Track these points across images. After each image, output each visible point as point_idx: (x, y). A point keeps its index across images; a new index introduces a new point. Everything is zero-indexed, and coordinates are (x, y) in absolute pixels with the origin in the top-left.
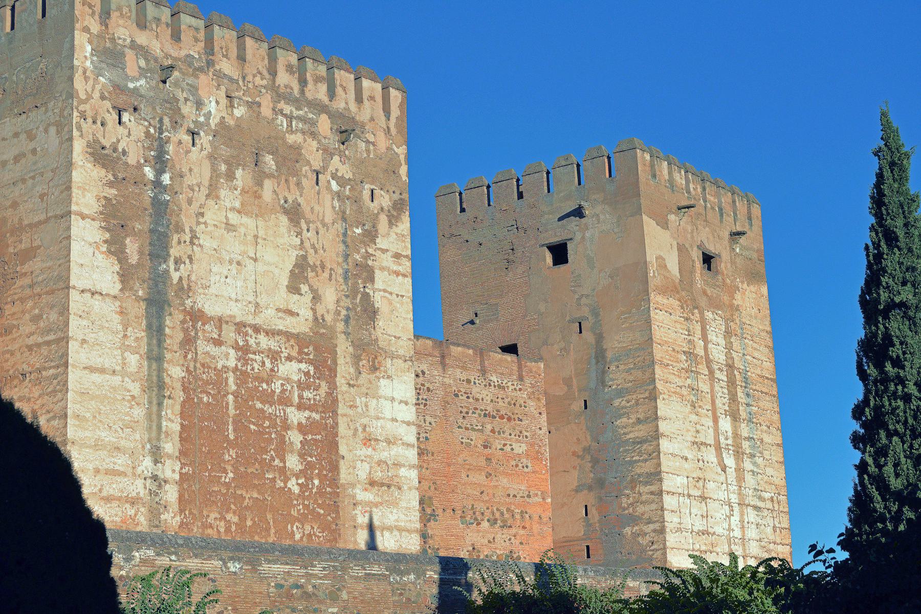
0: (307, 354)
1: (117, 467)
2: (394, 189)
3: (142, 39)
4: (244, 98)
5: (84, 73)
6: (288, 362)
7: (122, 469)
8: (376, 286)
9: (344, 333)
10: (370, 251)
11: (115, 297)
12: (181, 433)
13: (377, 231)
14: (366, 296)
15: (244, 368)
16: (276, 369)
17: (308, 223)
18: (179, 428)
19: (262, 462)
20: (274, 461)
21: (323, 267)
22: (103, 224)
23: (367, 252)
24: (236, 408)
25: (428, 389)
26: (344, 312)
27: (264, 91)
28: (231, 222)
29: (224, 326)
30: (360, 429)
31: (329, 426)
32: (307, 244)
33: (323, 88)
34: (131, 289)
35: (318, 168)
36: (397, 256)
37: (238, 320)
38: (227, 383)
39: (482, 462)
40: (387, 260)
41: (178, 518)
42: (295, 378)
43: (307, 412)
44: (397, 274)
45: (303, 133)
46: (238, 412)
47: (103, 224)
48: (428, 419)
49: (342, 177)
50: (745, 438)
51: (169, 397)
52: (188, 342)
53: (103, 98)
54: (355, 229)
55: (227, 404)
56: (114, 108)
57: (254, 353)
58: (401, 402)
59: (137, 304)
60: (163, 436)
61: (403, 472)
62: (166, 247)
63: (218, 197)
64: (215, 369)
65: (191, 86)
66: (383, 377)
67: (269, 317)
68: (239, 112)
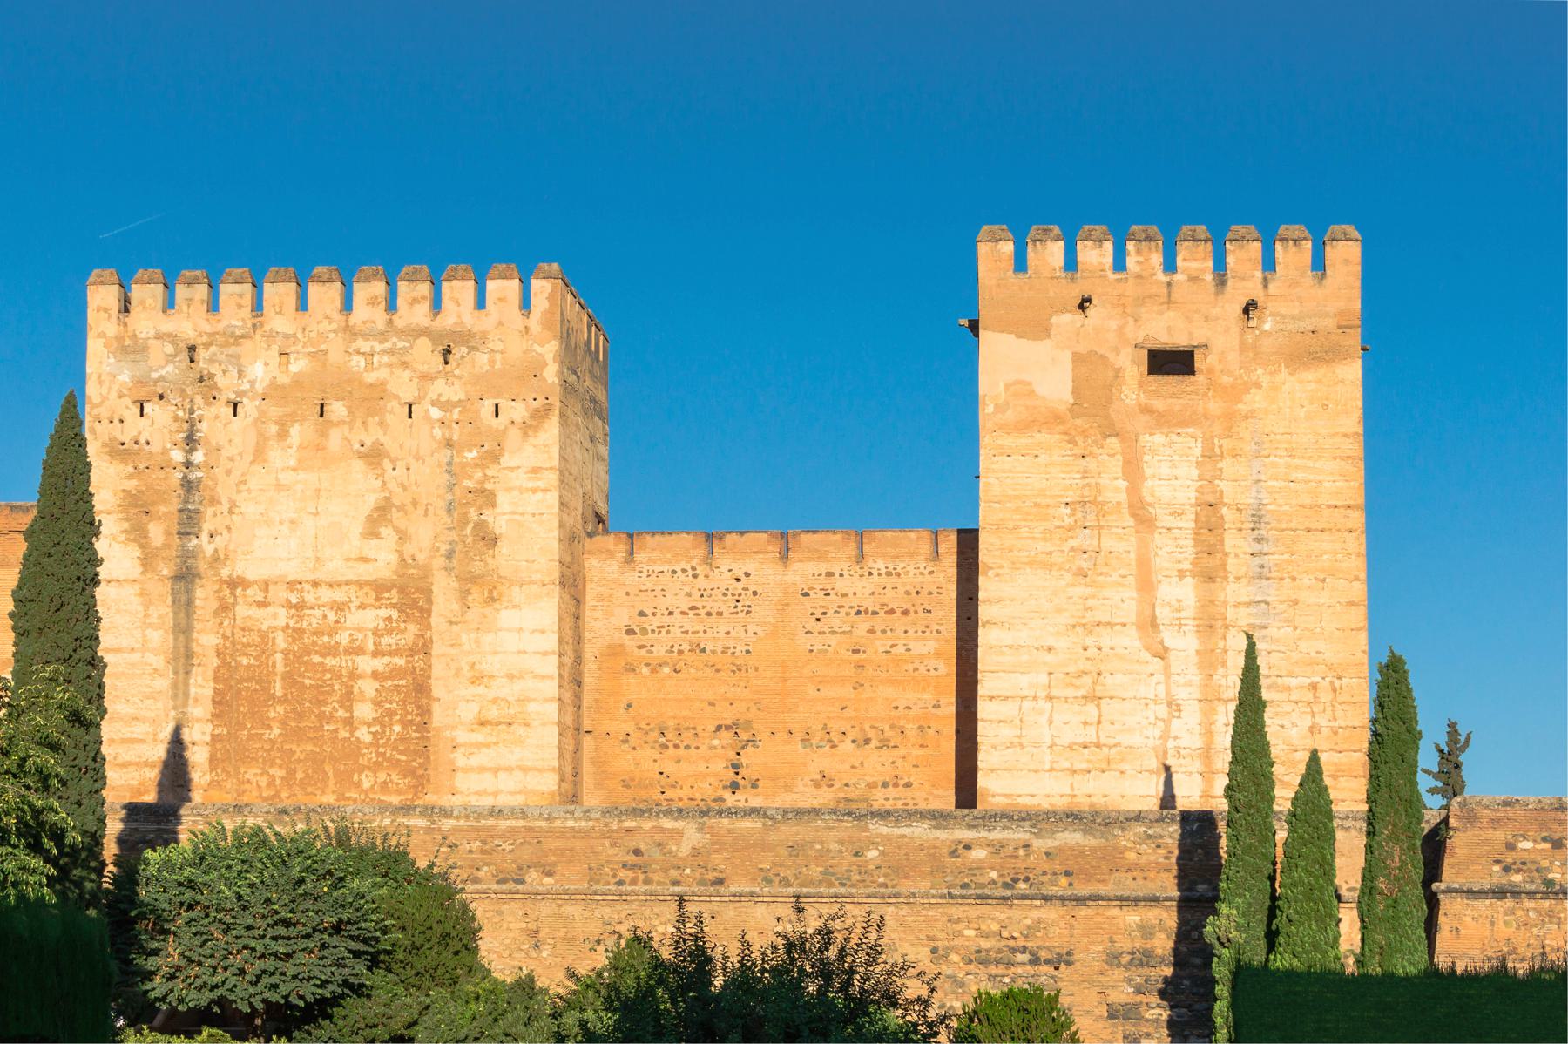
0: (388, 599)
1: (135, 736)
2: (534, 396)
3: (168, 325)
4: (304, 350)
5: (99, 377)
6: (361, 611)
7: (140, 737)
8: (498, 510)
9: (446, 569)
10: (489, 473)
11: (135, 581)
12: (213, 697)
13: (503, 449)
14: (481, 525)
15: (298, 625)
16: (342, 620)
17: (392, 461)
18: (209, 692)
19: (321, 717)
20: (337, 711)
21: (415, 503)
22: (121, 516)
23: (485, 475)
24: (286, 665)
25: (755, 593)
26: (444, 548)
27: (332, 335)
28: (283, 482)
29: (271, 588)
30: (466, 668)
31: (417, 670)
32: (392, 485)
33: (424, 308)
34: (154, 570)
35: (410, 400)
36: (535, 470)
37: (290, 578)
38: (274, 644)
39: (849, 671)
40: (521, 479)
41: (208, 778)
42: (371, 625)
43: (386, 657)
44: (534, 491)
45: (390, 366)
46: (288, 669)
47: (121, 516)
48: (751, 628)
49: (448, 401)
50: (1237, 605)
51: (199, 665)
52: (224, 608)
53: (121, 396)
54: (466, 454)
55: (274, 662)
56: (135, 402)
57: (312, 608)
58: (534, 631)
59: (161, 583)
60: (191, 701)
61: (532, 707)
62: (198, 524)
63: (265, 461)
64: (259, 631)
65: (231, 356)
66: (506, 608)
67: (336, 567)
68: (298, 365)
